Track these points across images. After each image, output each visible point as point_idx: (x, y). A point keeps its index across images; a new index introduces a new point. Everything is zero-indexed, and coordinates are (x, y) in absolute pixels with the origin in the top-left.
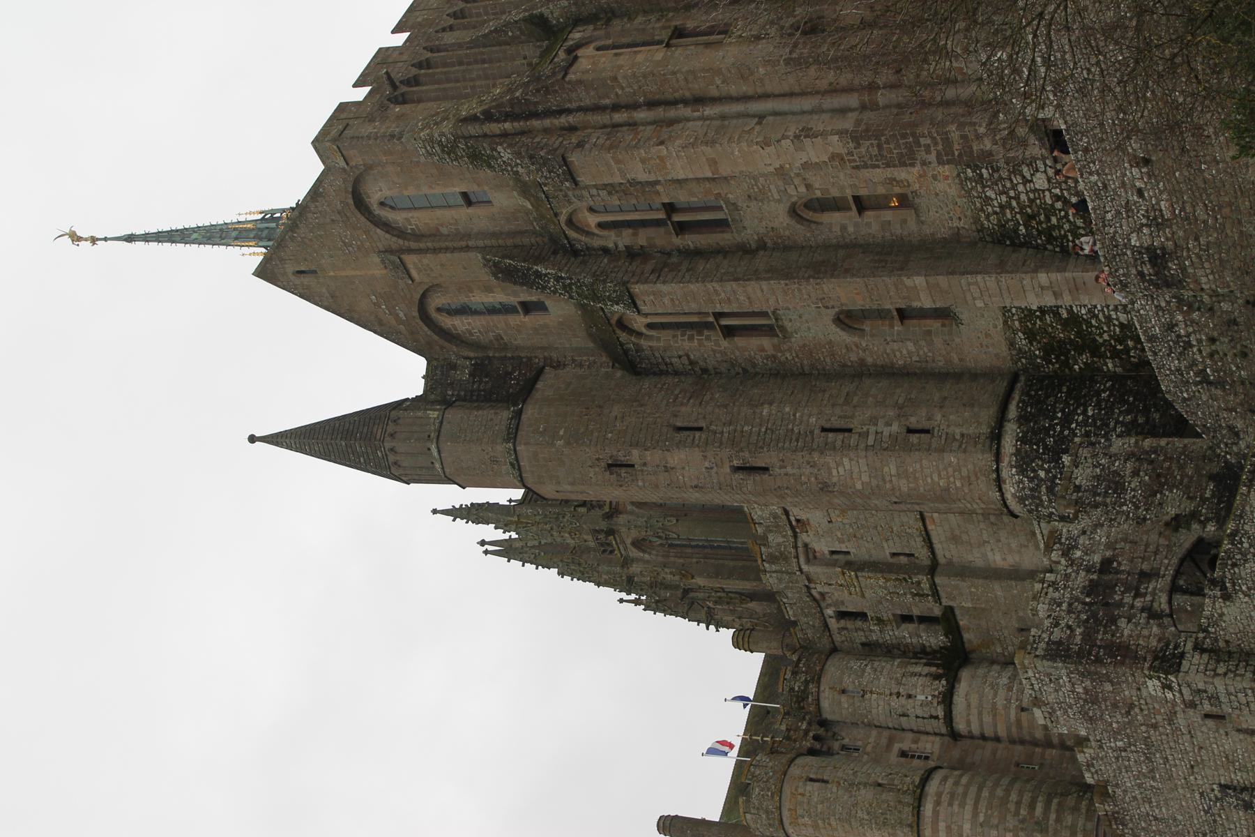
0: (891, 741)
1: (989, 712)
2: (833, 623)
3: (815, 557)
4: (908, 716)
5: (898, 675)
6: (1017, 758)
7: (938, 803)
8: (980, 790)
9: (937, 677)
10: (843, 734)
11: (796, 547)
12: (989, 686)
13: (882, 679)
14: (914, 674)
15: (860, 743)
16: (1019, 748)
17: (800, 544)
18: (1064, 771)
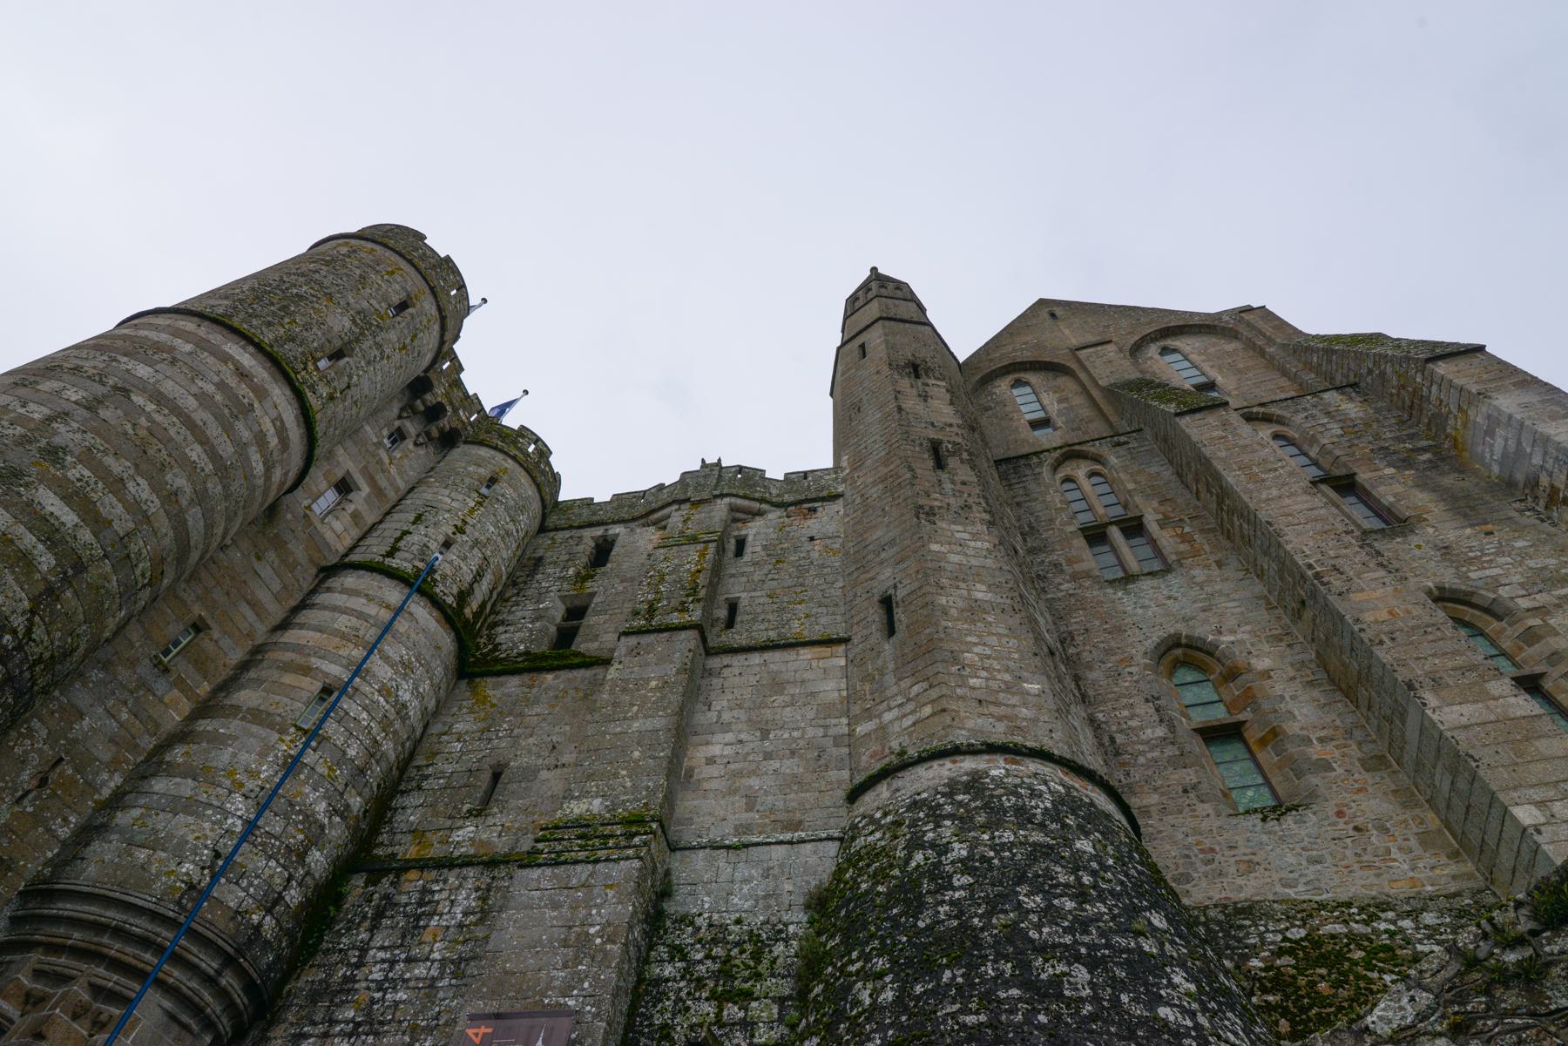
0: (378, 491)
1: (357, 630)
2: (599, 531)
3: (735, 520)
4: (414, 523)
5: (489, 553)
6: (216, 634)
7: (242, 374)
8: (214, 455)
9: (463, 597)
10: (422, 451)
11: (762, 500)
12: (410, 663)
13: (492, 529)
14: (479, 576)
15: (398, 454)
16: (236, 656)
17: (765, 506)
18: (110, 703)
